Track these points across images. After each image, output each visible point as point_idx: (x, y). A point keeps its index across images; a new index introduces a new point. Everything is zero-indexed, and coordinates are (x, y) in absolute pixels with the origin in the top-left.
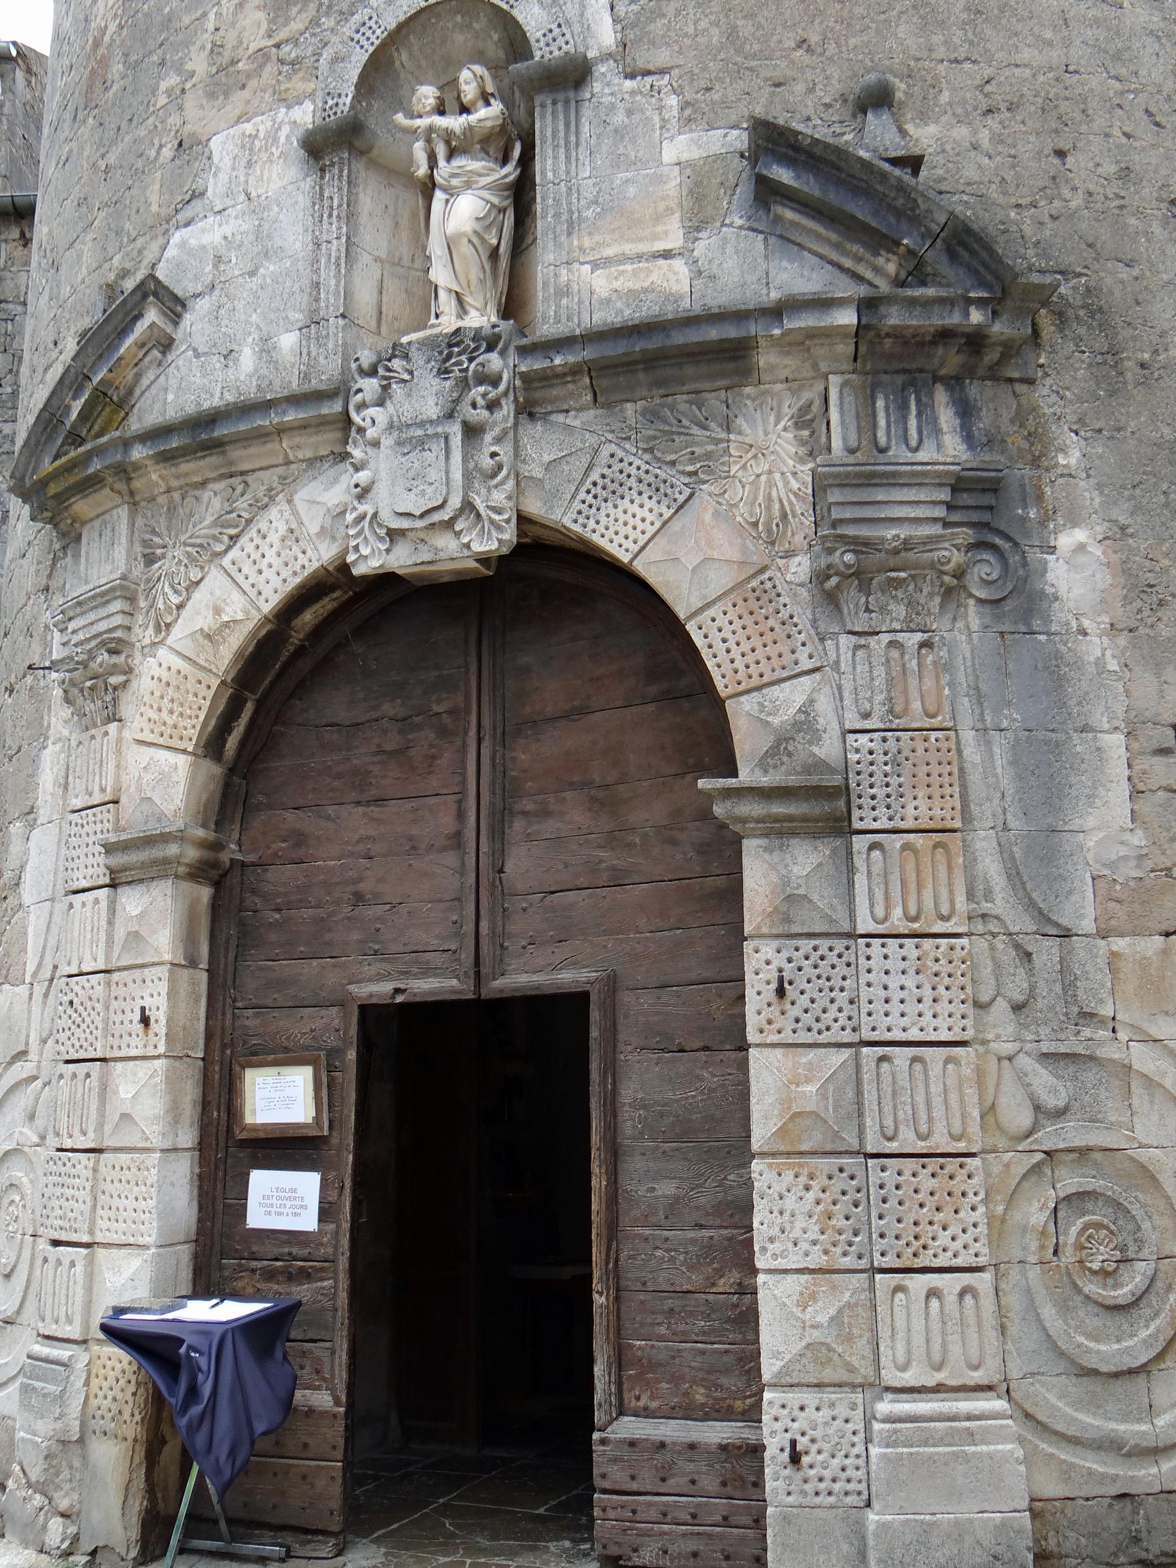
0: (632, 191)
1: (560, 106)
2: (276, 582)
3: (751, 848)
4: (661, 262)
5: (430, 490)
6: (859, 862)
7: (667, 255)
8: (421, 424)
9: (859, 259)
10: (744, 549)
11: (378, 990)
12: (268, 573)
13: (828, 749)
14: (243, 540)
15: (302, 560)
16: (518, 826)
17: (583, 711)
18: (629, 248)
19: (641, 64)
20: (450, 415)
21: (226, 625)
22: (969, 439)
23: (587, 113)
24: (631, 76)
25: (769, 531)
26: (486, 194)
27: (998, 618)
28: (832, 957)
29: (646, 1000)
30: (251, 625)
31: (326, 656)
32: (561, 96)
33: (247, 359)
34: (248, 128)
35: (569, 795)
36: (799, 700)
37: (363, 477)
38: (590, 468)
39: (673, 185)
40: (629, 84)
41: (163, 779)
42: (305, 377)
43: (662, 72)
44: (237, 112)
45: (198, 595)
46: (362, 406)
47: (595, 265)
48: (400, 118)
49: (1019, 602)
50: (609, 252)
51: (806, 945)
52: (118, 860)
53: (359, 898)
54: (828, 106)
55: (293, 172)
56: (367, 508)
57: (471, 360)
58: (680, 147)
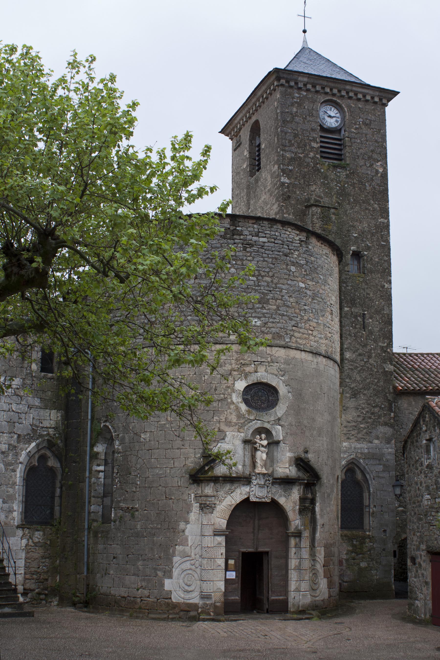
11: (244, 550)
41: (223, 523)
42: (243, 473)
55: (240, 442)
58: (289, 454)
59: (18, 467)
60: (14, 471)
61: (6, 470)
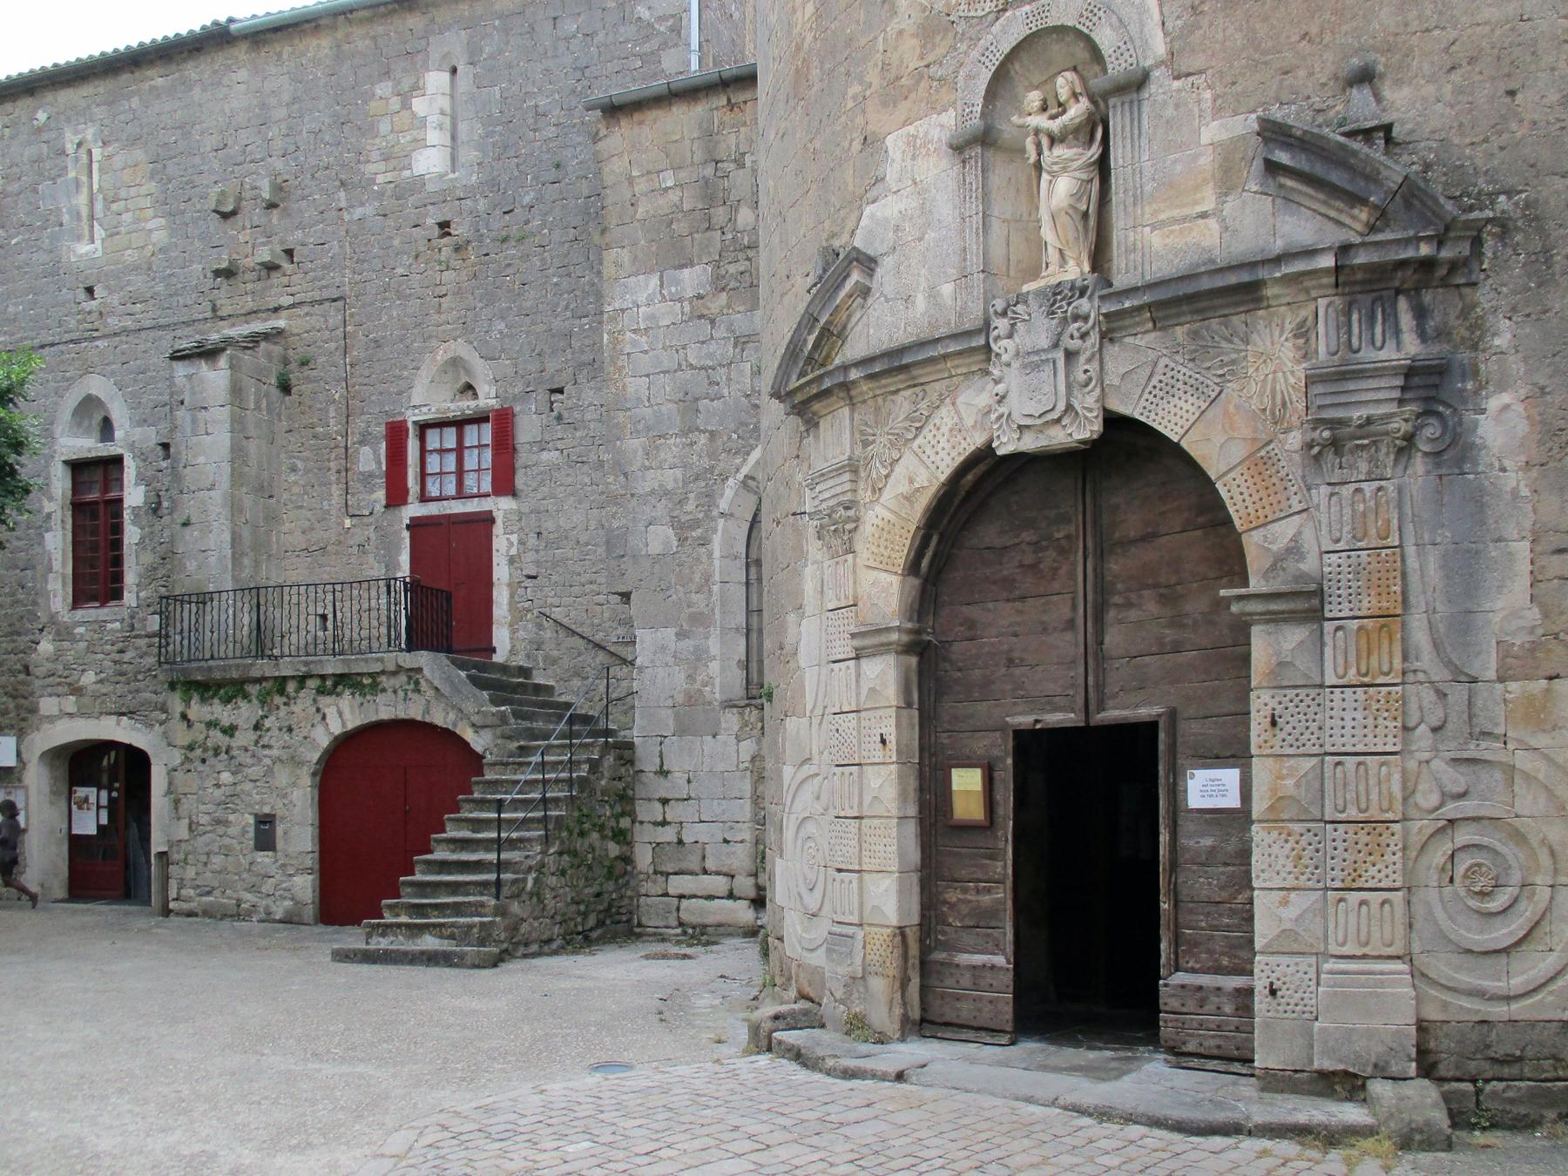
0: (1179, 168)
1: (1127, 107)
2: (948, 460)
3: (1257, 632)
4: (1200, 221)
5: (1044, 399)
6: (1328, 639)
7: (1204, 215)
8: (1037, 352)
9: (1340, 211)
10: (1255, 430)
12: (943, 454)
13: (1309, 565)
14: (925, 431)
15: (964, 444)
16: (1111, 614)
17: (1155, 535)
18: (1176, 213)
19: (1184, 69)
20: (1056, 345)
21: (917, 490)
22: (1422, 336)
23: (1146, 108)
24: (1177, 78)
25: (1273, 413)
26: (1077, 174)
27: (1438, 465)
28: (1308, 701)
29: (1195, 727)
30: (933, 490)
31: (983, 490)
32: (1127, 98)
33: (921, 302)
34: (911, 129)
35: (1146, 593)
36: (1291, 533)
37: (1000, 388)
38: (1151, 376)
39: (1206, 161)
40: (1176, 84)
43: (1200, 72)
44: (903, 118)
45: (898, 469)
46: (997, 338)
47: (1154, 228)
48: (1015, 119)
49: (1455, 453)
50: (1162, 217)
51: (1291, 693)
52: (857, 643)
53: (1010, 663)
54: (1324, 85)
55: (945, 163)
56: (1003, 409)
57: (1069, 304)
58: (1213, 132)
59: (715, 531)
60: (704, 542)
61: (682, 540)
